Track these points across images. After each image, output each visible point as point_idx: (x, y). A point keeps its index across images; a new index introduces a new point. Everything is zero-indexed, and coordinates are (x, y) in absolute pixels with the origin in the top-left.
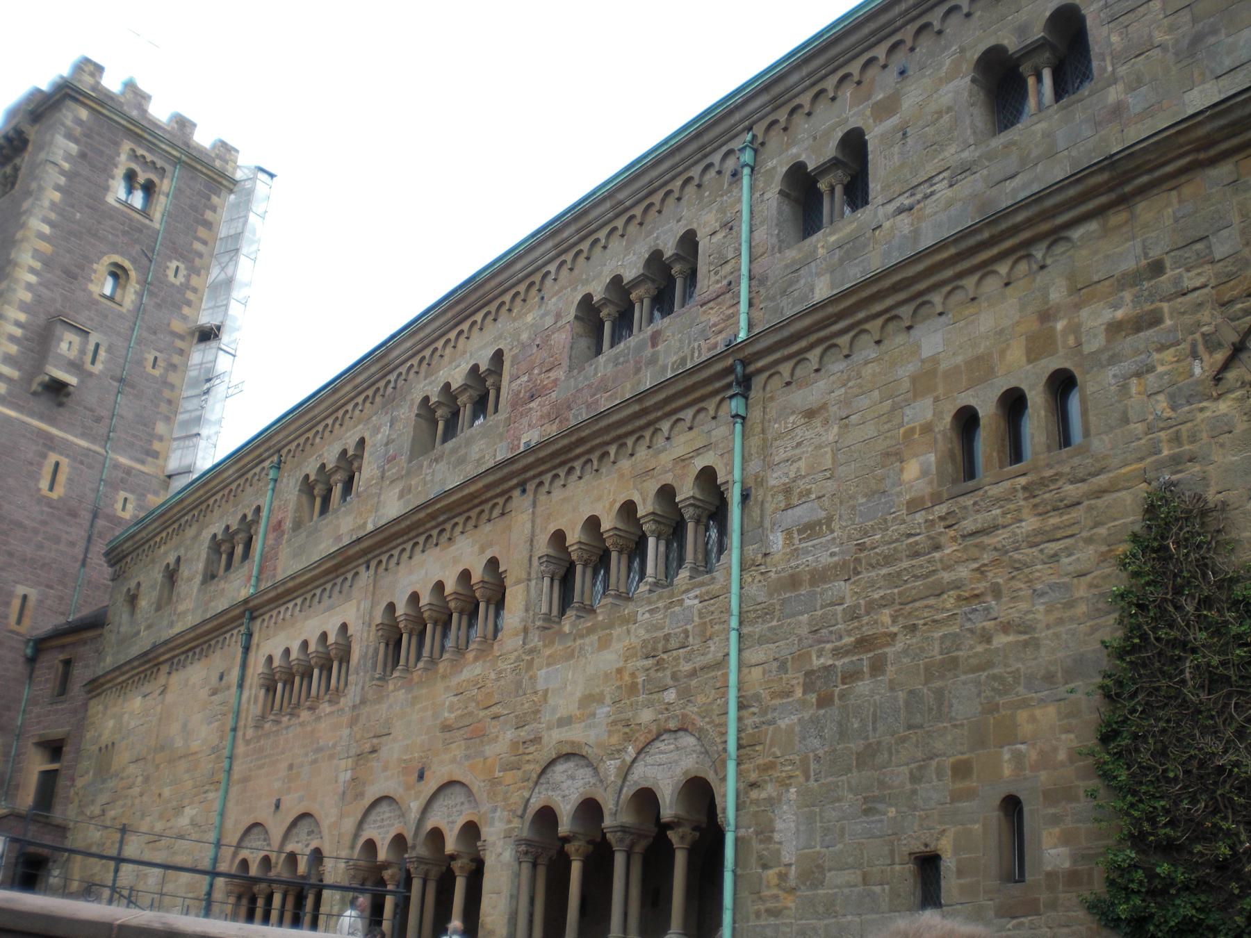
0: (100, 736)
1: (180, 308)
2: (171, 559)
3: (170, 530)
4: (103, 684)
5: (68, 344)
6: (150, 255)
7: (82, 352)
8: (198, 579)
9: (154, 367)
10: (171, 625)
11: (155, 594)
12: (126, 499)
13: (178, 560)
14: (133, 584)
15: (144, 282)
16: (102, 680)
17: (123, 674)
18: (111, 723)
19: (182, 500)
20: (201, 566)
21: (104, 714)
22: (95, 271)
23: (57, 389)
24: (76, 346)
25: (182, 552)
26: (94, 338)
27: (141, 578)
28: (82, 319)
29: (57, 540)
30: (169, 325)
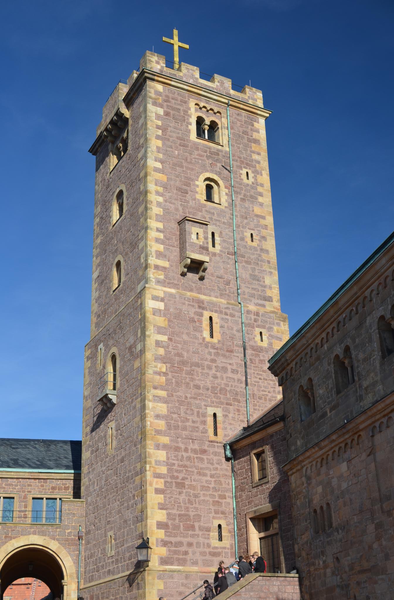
0: (310, 501)
1: (257, 199)
2: (339, 350)
3: (329, 330)
4: (302, 461)
5: (195, 235)
6: (228, 168)
7: (206, 238)
8: (377, 356)
9: (252, 241)
10: (361, 398)
11: (331, 383)
12: (261, 333)
13: (347, 349)
14: (304, 381)
15: (230, 187)
16: (300, 459)
17: (321, 449)
18: (320, 489)
19: (336, 303)
20: (376, 345)
21: (309, 484)
22: (198, 186)
23: (196, 266)
24: (201, 235)
25: (349, 342)
26: (211, 228)
27: (312, 375)
28: (199, 217)
29: (225, 369)
30: (253, 211)
